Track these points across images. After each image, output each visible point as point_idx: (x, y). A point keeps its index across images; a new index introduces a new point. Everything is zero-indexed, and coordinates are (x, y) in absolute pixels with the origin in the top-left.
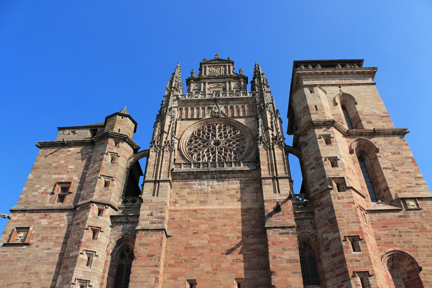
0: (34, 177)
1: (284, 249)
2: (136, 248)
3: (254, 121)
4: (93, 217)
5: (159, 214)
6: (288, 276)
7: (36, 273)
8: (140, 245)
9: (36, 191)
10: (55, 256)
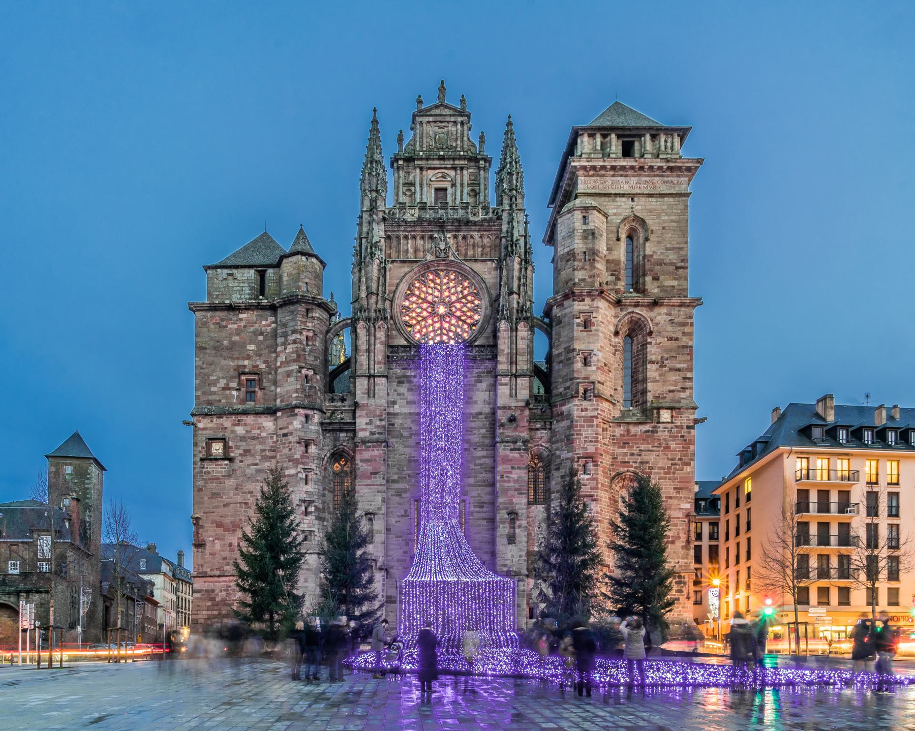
0: (203, 364)
1: (513, 468)
2: (358, 464)
3: (496, 269)
4: (303, 427)
5: (378, 423)
6: (513, 496)
7: (251, 492)
8: (362, 461)
9: (215, 385)
10: (266, 472)
